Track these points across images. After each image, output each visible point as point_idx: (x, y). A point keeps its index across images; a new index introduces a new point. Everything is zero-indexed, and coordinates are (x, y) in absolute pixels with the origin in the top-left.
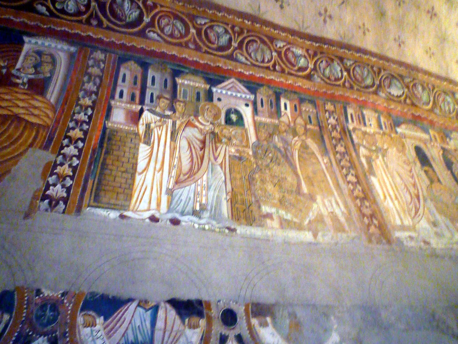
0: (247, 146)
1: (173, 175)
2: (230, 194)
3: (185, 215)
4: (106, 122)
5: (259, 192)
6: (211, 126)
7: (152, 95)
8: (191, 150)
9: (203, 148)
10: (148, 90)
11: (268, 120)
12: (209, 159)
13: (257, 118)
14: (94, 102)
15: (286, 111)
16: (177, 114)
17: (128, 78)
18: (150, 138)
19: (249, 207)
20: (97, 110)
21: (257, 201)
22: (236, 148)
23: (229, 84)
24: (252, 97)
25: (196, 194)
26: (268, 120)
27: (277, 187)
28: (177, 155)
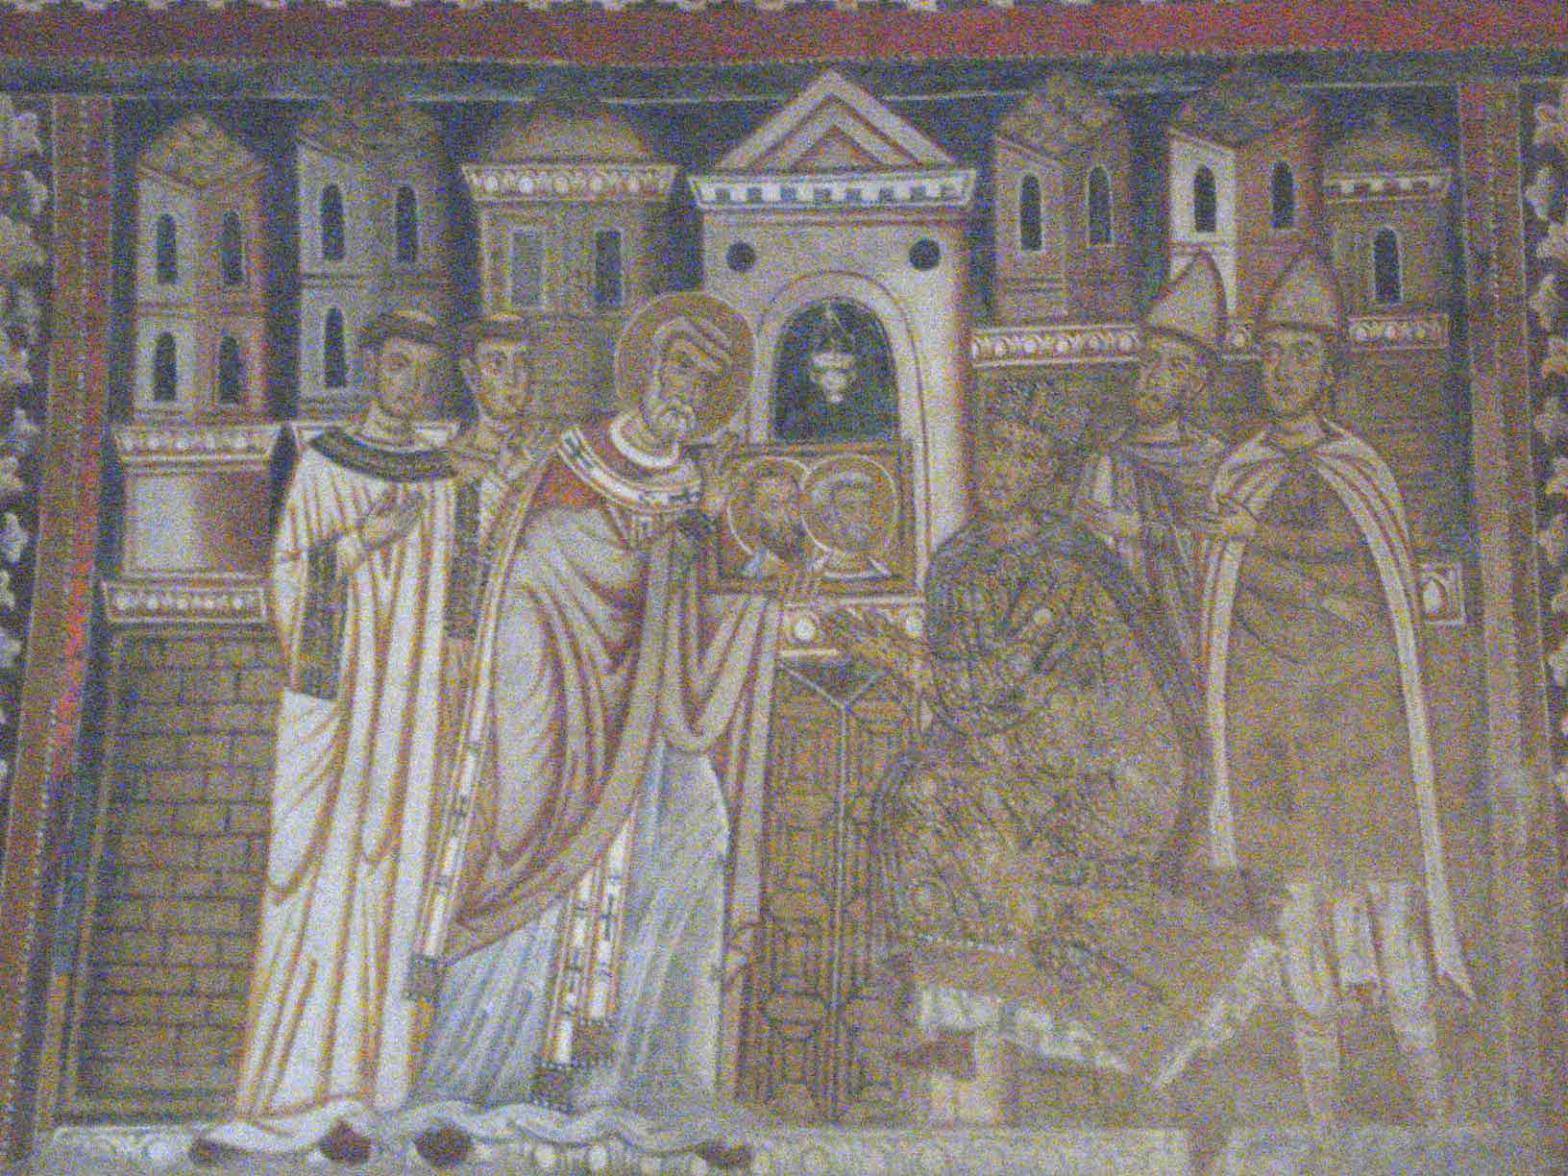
0: (896, 582)
1: (447, 871)
2: (746, 938)
3: (496, 1105)
4: (104, 585)
5: (924, 897)
6: (687, 468)
7: (334, 322)
8: (559, 681)
9: (624, 652)
10: (304, 292)
11: (1063, 344)
12: (657, 722)
13: (988, 342)
14: (28, 470)
15: (1203, 237)
16: (485, 438)
17: (188, 245)
18: (332, 648)
19: (840, 1007)
20: (53, 514)
21: (899, 965)
22: (827, 605)
23: (804, 121)
24: (961, 183)
25: (565, 965)
26: (1063, 344)
27: (1042, 848)
28: (476, 734)
